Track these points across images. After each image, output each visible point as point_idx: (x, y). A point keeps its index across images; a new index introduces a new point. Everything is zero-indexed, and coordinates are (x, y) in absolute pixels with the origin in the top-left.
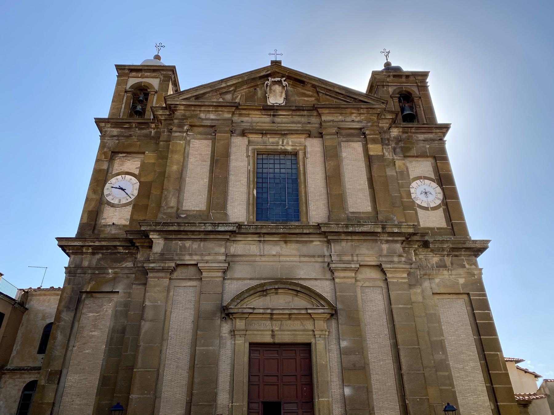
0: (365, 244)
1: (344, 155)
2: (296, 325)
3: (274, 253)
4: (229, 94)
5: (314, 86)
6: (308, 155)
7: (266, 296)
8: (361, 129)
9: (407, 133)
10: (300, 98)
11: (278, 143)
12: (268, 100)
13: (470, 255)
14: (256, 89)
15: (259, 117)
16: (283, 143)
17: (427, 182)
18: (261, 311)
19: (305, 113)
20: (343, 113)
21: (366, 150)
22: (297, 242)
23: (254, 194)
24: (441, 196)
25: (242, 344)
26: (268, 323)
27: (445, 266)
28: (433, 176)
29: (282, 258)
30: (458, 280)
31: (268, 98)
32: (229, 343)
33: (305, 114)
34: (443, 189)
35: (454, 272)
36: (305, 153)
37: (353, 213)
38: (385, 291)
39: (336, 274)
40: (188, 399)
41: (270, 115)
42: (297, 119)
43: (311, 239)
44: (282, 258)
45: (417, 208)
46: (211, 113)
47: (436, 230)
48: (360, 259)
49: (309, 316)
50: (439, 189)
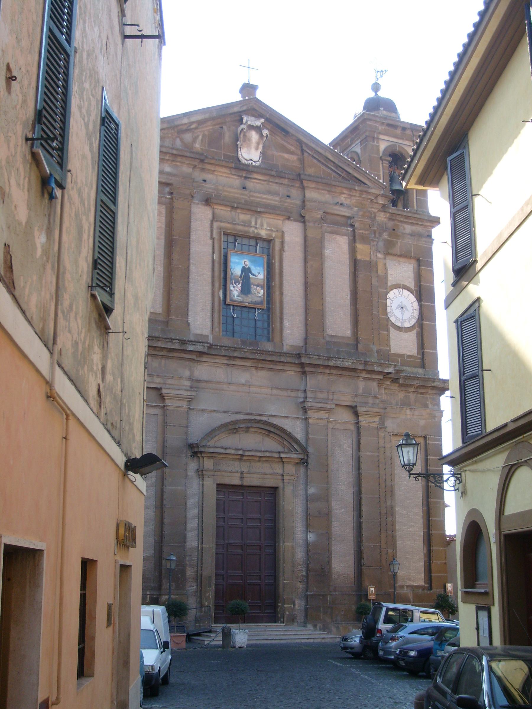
0: (342, 379)
1: (327, 252)
2: (265, 467)
3: (243, 381)
4: (189, 133)
5: (300, 142)
6: (286, 248)
7: (235, 433)
8: (349, 218)
9: (393, 220)
10: (279, 154)
11: (250, 222)
12: (239, 153)
13: (436, 394)
14: (222, 128)
15: (226, 177)
16: (256, 224)
17: (406, 292)
18: (233, 452)
19: (286, 181)
20: (331, 191)
21: (353, 251)
22: (270, 369)
23: (220, 297)
24: (416, 314)
25: (210, 485)
26: (237, 463)
27: (409, 405)
28: (412, 286)
29: (253, 389)
30: (419, 422)
31: (241, 148)
32: (194, 482)
33: (286, 183)
34: (420, 306)
35: (416, 413)
36: (282, 243)
37: (331, 336)
38: (354, 435)
39: (310, 414)
40: (156, 539)
41: (241, 176)
42: (274, 187)
43: (285, 368)
44: (253, 389)
45: (390, 327)
46: (165, 161)
47: (406, 359)
48: (335, 397)
49: (279, 460)
50: (416, 305)
